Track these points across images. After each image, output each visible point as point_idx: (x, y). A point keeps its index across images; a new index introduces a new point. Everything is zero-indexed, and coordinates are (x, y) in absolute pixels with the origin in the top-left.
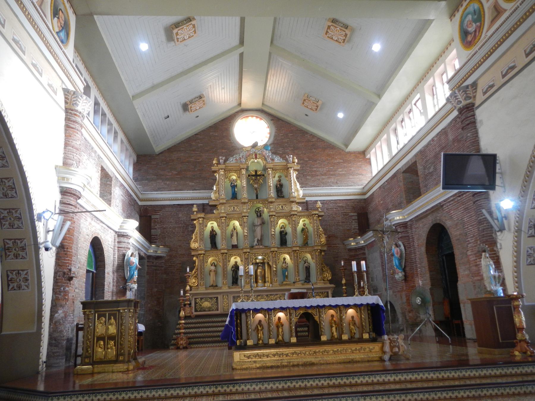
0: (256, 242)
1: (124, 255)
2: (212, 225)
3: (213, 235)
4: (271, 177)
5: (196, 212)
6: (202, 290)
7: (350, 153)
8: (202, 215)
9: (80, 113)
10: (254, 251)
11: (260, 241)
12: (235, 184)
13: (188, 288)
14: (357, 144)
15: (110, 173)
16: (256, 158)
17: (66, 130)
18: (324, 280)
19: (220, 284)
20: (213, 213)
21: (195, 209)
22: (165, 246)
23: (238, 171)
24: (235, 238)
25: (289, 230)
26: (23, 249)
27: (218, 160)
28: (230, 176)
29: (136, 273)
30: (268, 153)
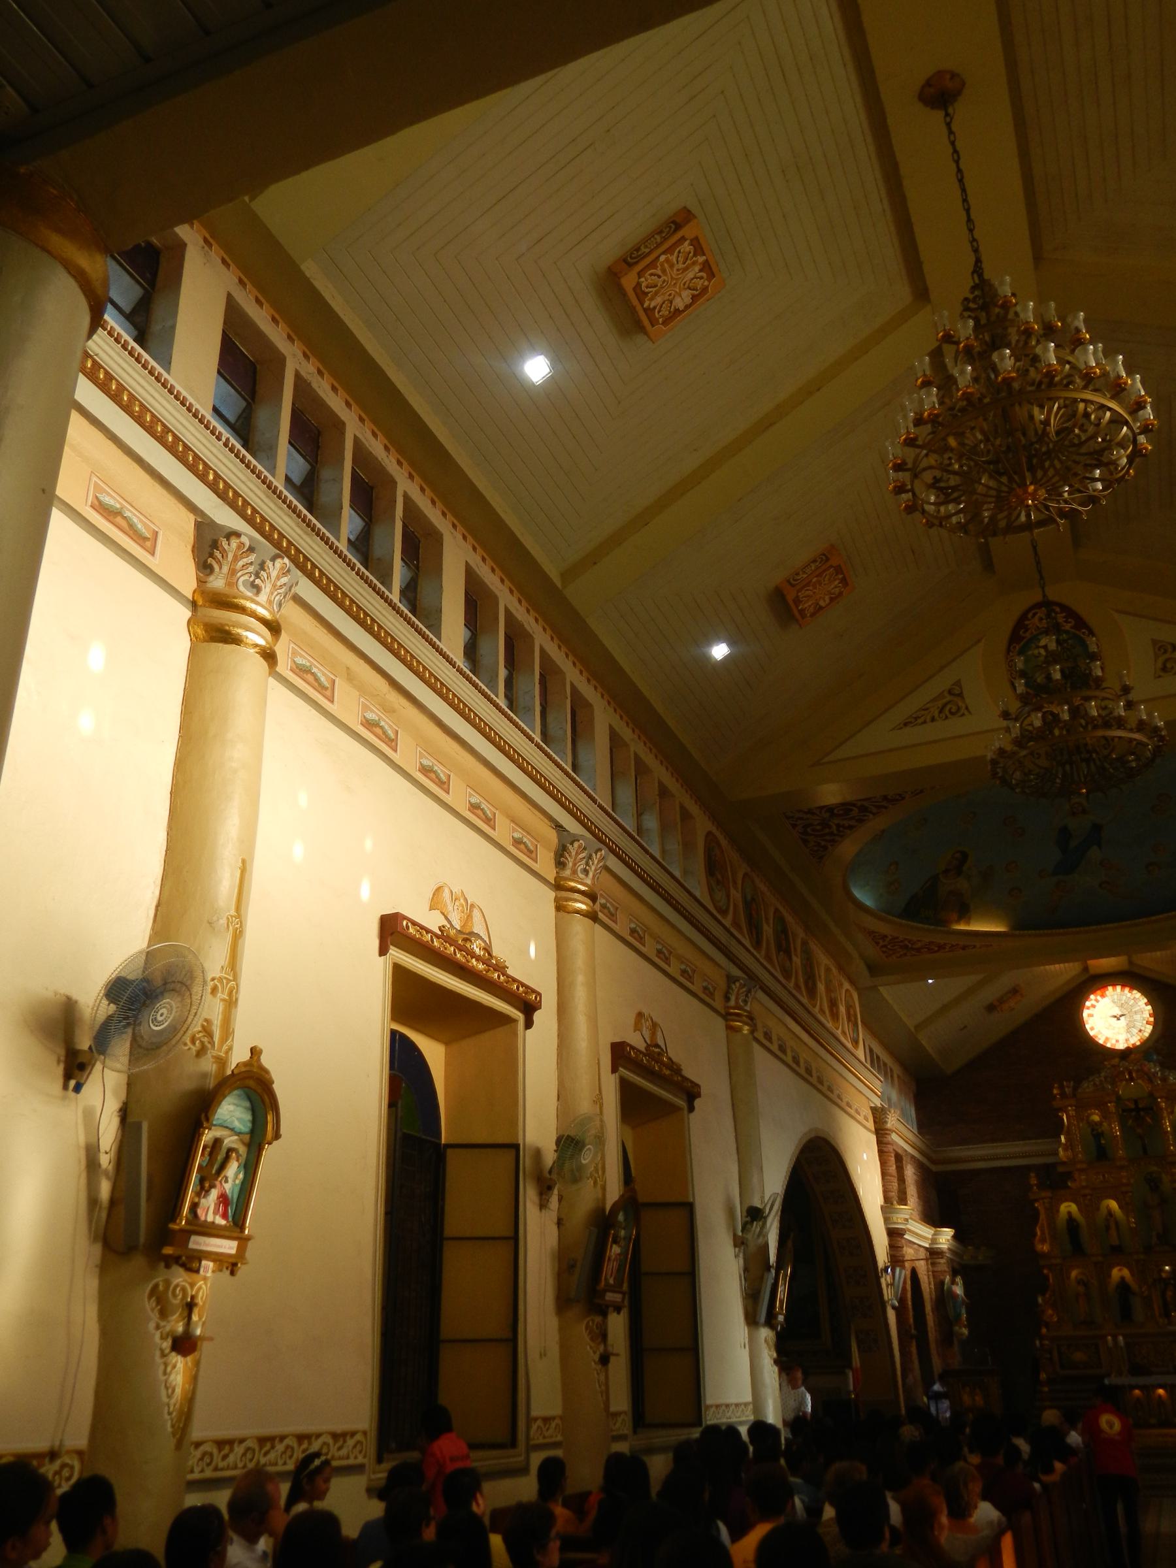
1: (942, 1283)
2: (1068, 1208)
4: (1165, 1114)
5: (1036, 1185)
8: (1049, 1194)
9: (890, 1130)
12: (1100, 1130)
13: (1044, 1330)
15: (900, 1151)
16: (1132, 1079)
17: (880, 1156)
20: (1069, 1187)
21: (1034, 1181)
23: (1101, 1106)
24: (1113, 1232)
27: (1061, 1087)
28: (1088, 1116)
29: (964, 1311)
30: (1155, 1069)
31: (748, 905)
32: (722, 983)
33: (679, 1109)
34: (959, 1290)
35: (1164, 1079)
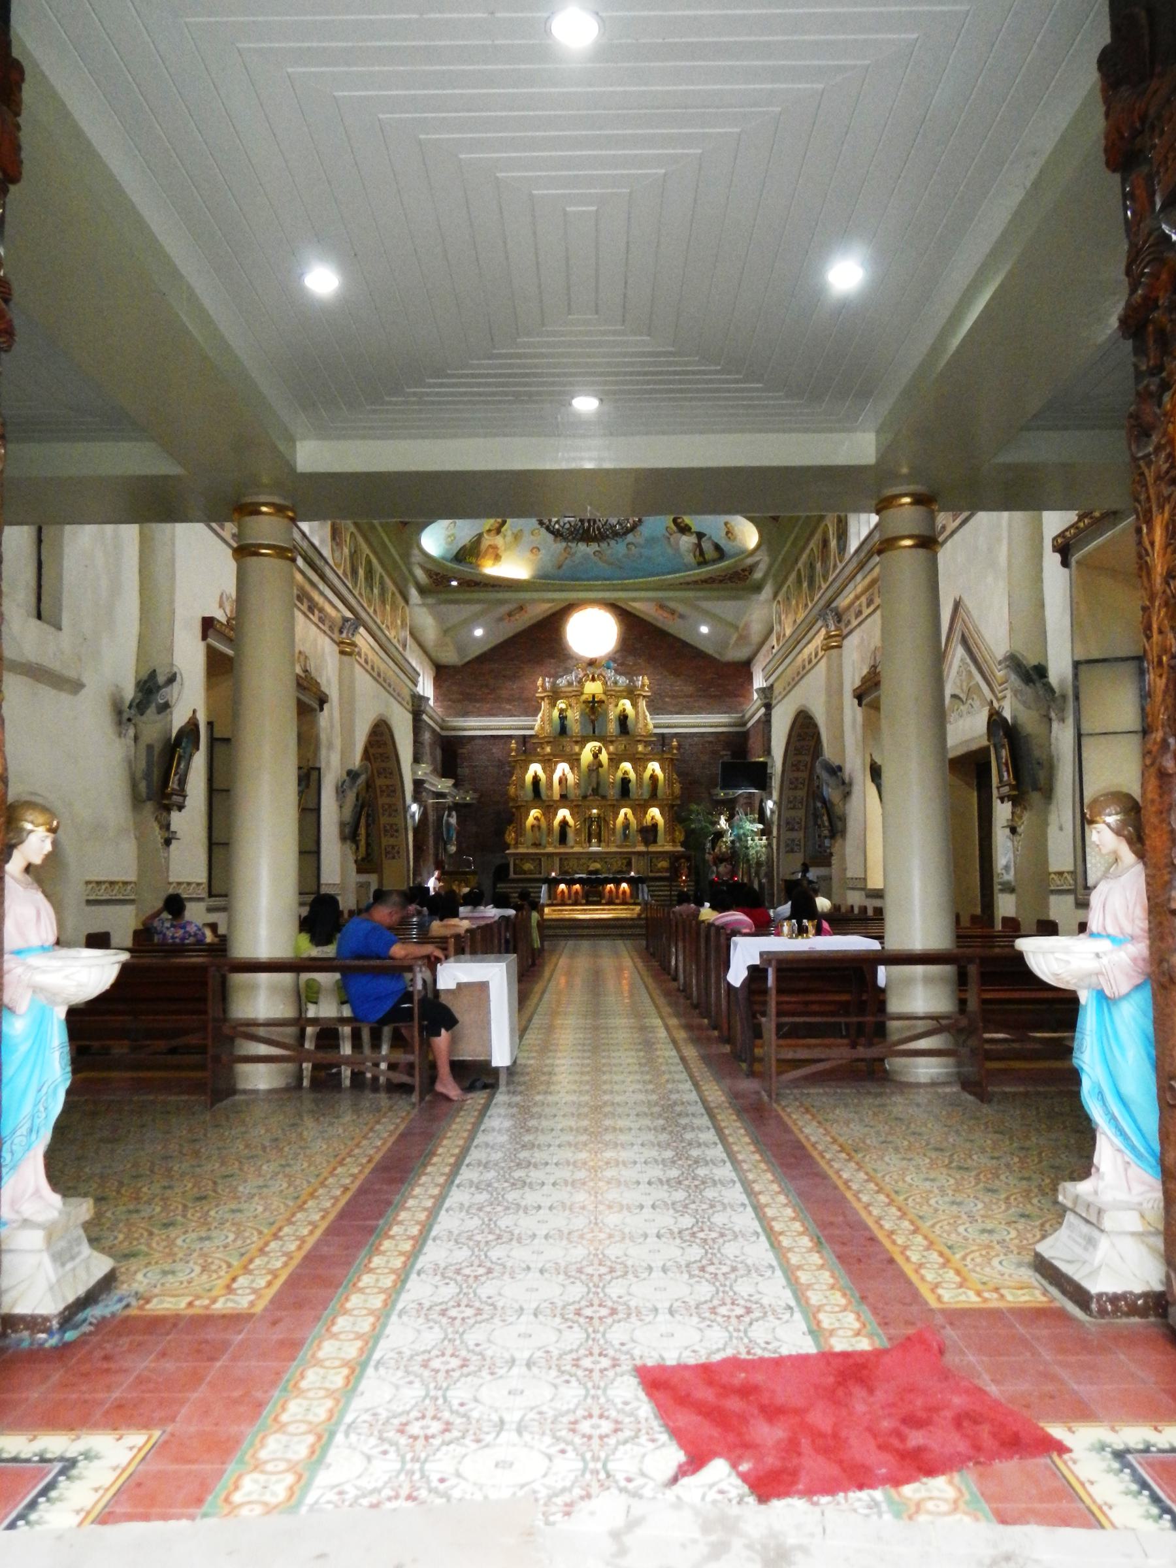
0: (590, 792)
2: (535, 769)
3: (536, 780)
6: (522, 850)
7: (729, 664)
10: (587, 803)
11: (596, 791)
14: (736, 654)
16: (593, 679)
18: (673, 841)
19: (544, 842)
21: (513, 745)
22: (475, 791)
25: (632, 775)
26: (397, 831)
27: (544, 680)
30: (610, 674)
31: (354, 555)
32: (339, 622)
33: (313, 710)
34: (453, 821)
35: (616, 683)
